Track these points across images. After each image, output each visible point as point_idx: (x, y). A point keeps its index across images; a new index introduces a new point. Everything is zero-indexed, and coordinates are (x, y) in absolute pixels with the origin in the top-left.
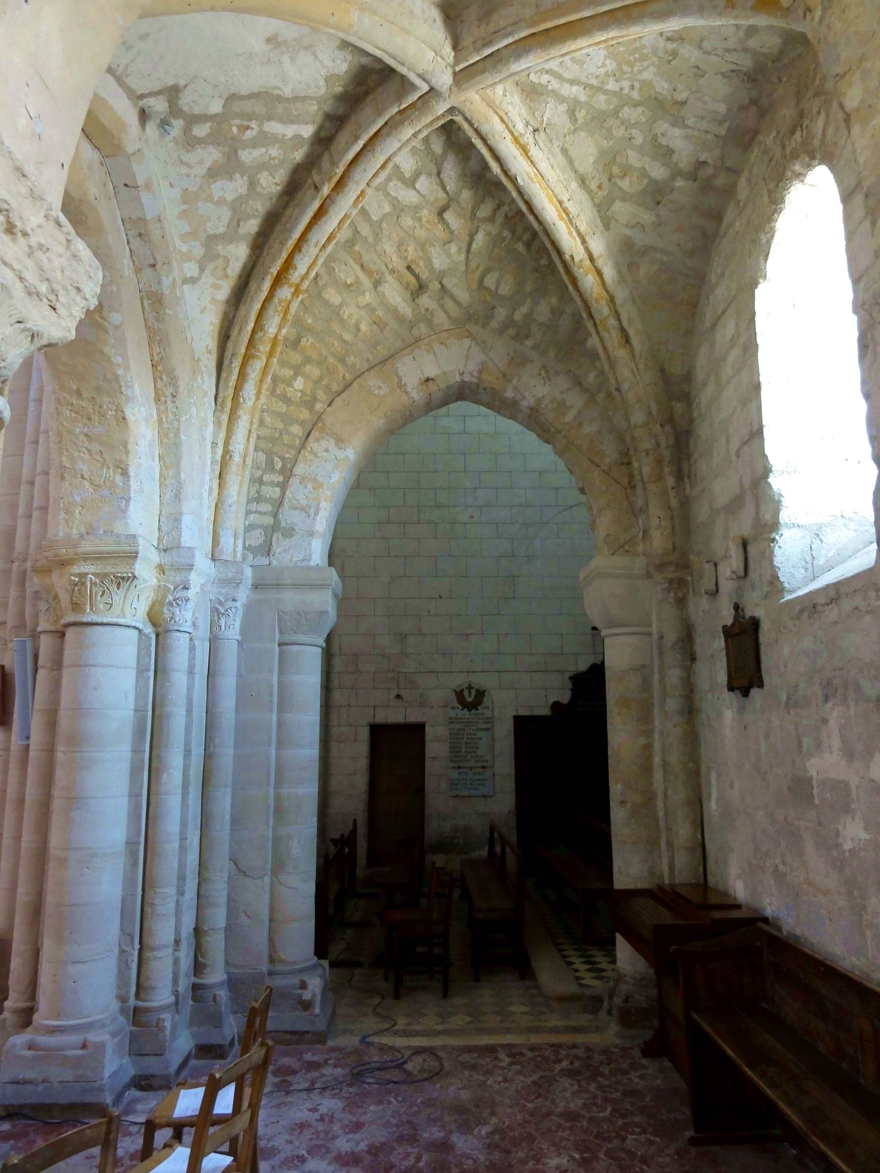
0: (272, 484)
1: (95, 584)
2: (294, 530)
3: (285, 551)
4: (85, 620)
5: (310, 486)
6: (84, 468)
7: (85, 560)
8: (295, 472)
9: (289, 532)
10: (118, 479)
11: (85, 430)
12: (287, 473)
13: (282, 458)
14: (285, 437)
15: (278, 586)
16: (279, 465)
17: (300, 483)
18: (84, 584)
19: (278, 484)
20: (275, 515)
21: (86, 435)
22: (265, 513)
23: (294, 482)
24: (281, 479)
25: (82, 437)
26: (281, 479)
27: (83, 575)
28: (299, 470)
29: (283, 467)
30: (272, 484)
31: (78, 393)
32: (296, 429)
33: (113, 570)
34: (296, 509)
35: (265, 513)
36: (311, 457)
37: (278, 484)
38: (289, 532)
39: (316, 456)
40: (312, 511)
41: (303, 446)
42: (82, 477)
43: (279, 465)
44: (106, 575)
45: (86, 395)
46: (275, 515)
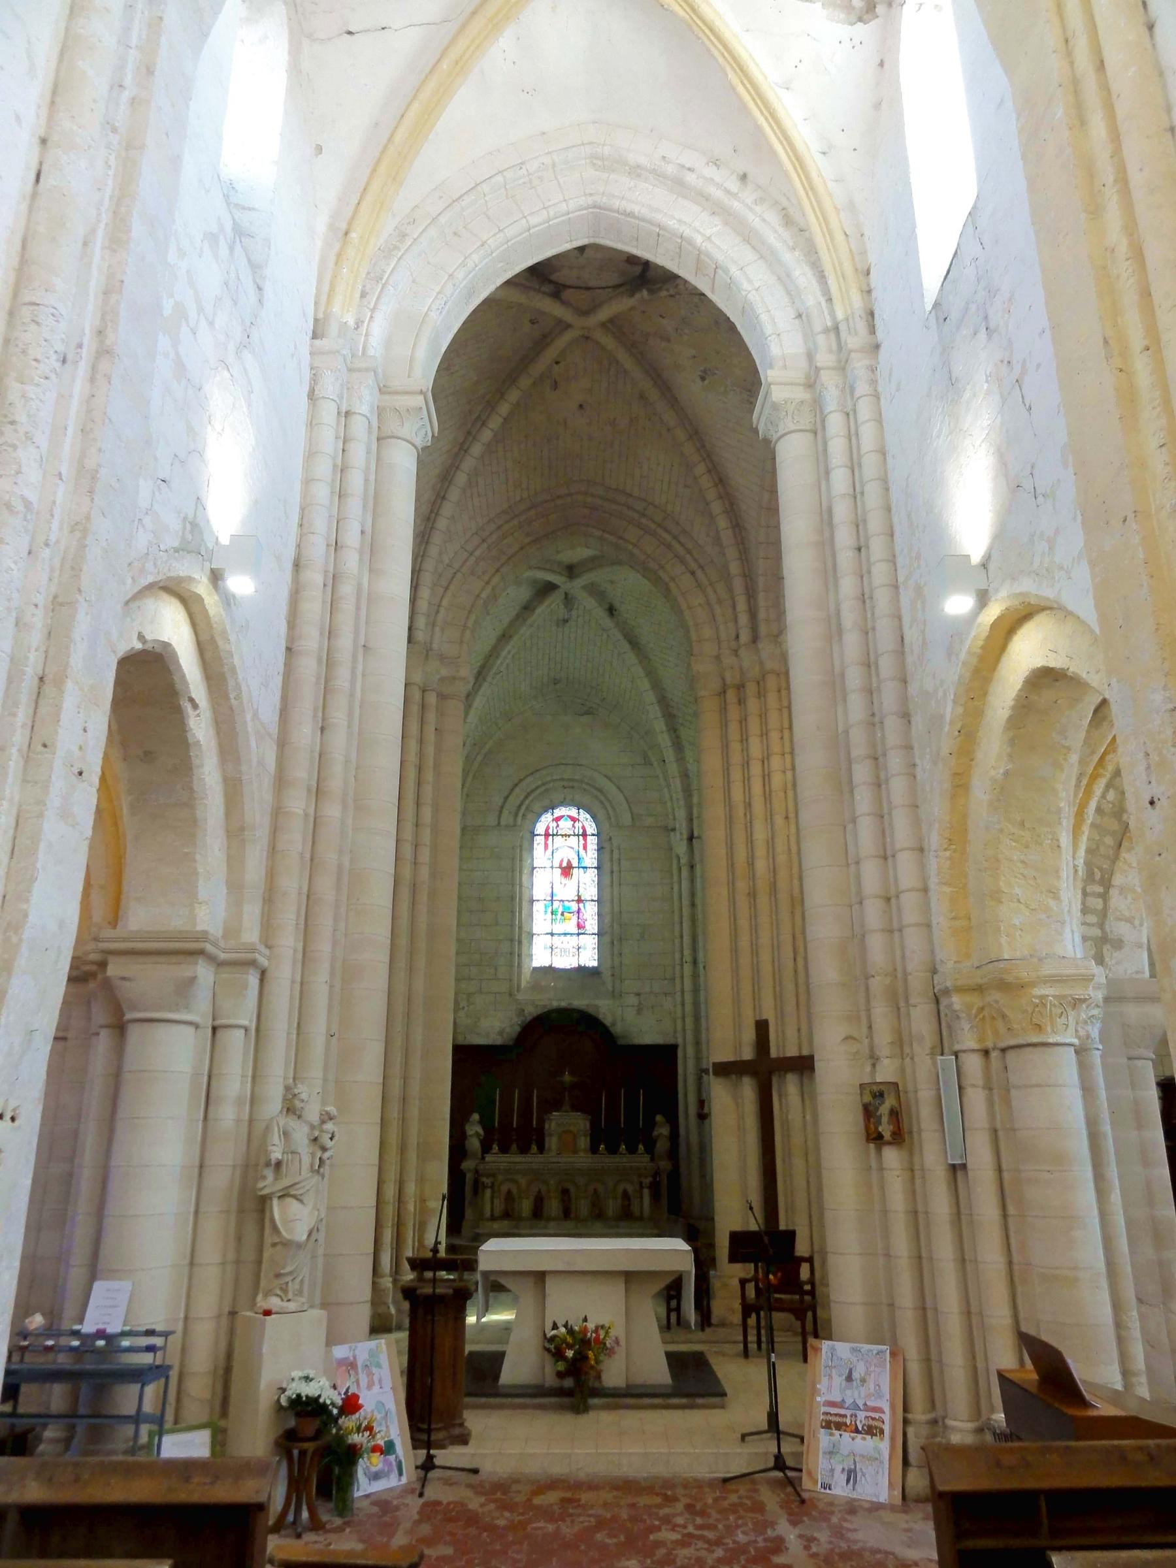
0: (1094, 895)
1: (1055, 1006)
2: (1121, 941)
3: (1117, 963)
4: (1051, 1041)
5: (1129, 897)
6: (1017, 890)
7: (1045, 982)
8: (1113, 883)
9: (1118, 944)
10: (1052, 903)
11: (1022, 857)
12: (1107, 883)
13: (1101, 869)
14: (1102, 849)
15: (1121, 999)
16: (1098, 875)
17: (1120, 894)
18: (1045, 1005)
19: (1100, 895)
20: (1101, 926)
21: (1023, 862)
22: (1093, 925)
23: (1114, 893)
24: (1101, 889)
25: (1019, 864)
26: (1101, 889)
27: (1042, 997)
28: (1118, 880)
29: (1102, 877)
30: (1094, 895)
31: (1022, 824)
32: (1109, 841)
33: (1070, 992)
34: (1121, 920)
35: (1093, 925)
36: (1126, 867)
37: (1100, 895)
38: (1118, 944)
39: (1130, 866)
40: (1137, 922)
41: (1116, 857)
42: (1019, 901)
43: (1098, 875)
44: (1064, 997)
45: (1027, 825)
46: (1101, 926)
